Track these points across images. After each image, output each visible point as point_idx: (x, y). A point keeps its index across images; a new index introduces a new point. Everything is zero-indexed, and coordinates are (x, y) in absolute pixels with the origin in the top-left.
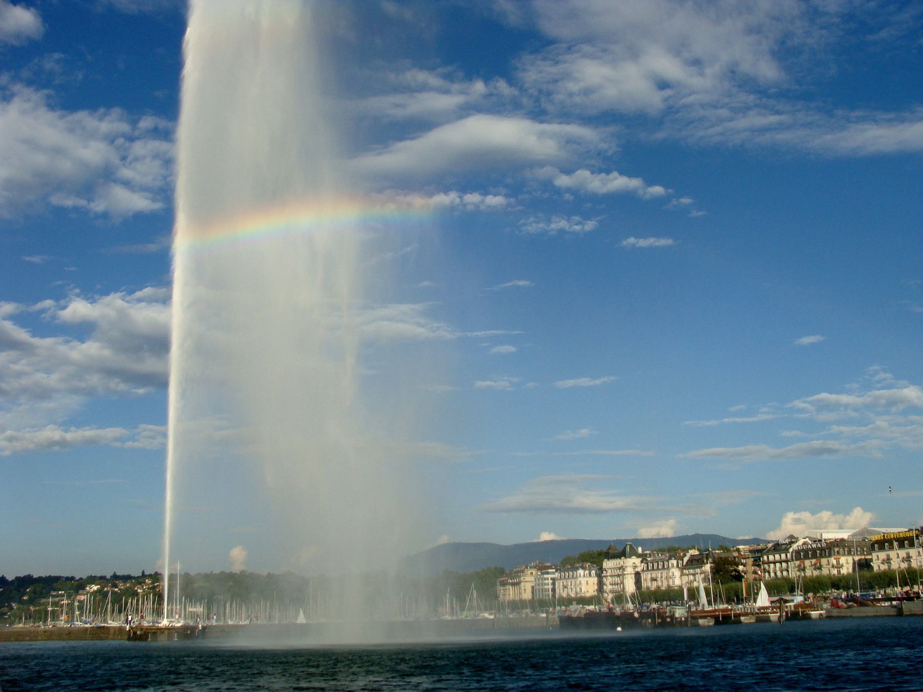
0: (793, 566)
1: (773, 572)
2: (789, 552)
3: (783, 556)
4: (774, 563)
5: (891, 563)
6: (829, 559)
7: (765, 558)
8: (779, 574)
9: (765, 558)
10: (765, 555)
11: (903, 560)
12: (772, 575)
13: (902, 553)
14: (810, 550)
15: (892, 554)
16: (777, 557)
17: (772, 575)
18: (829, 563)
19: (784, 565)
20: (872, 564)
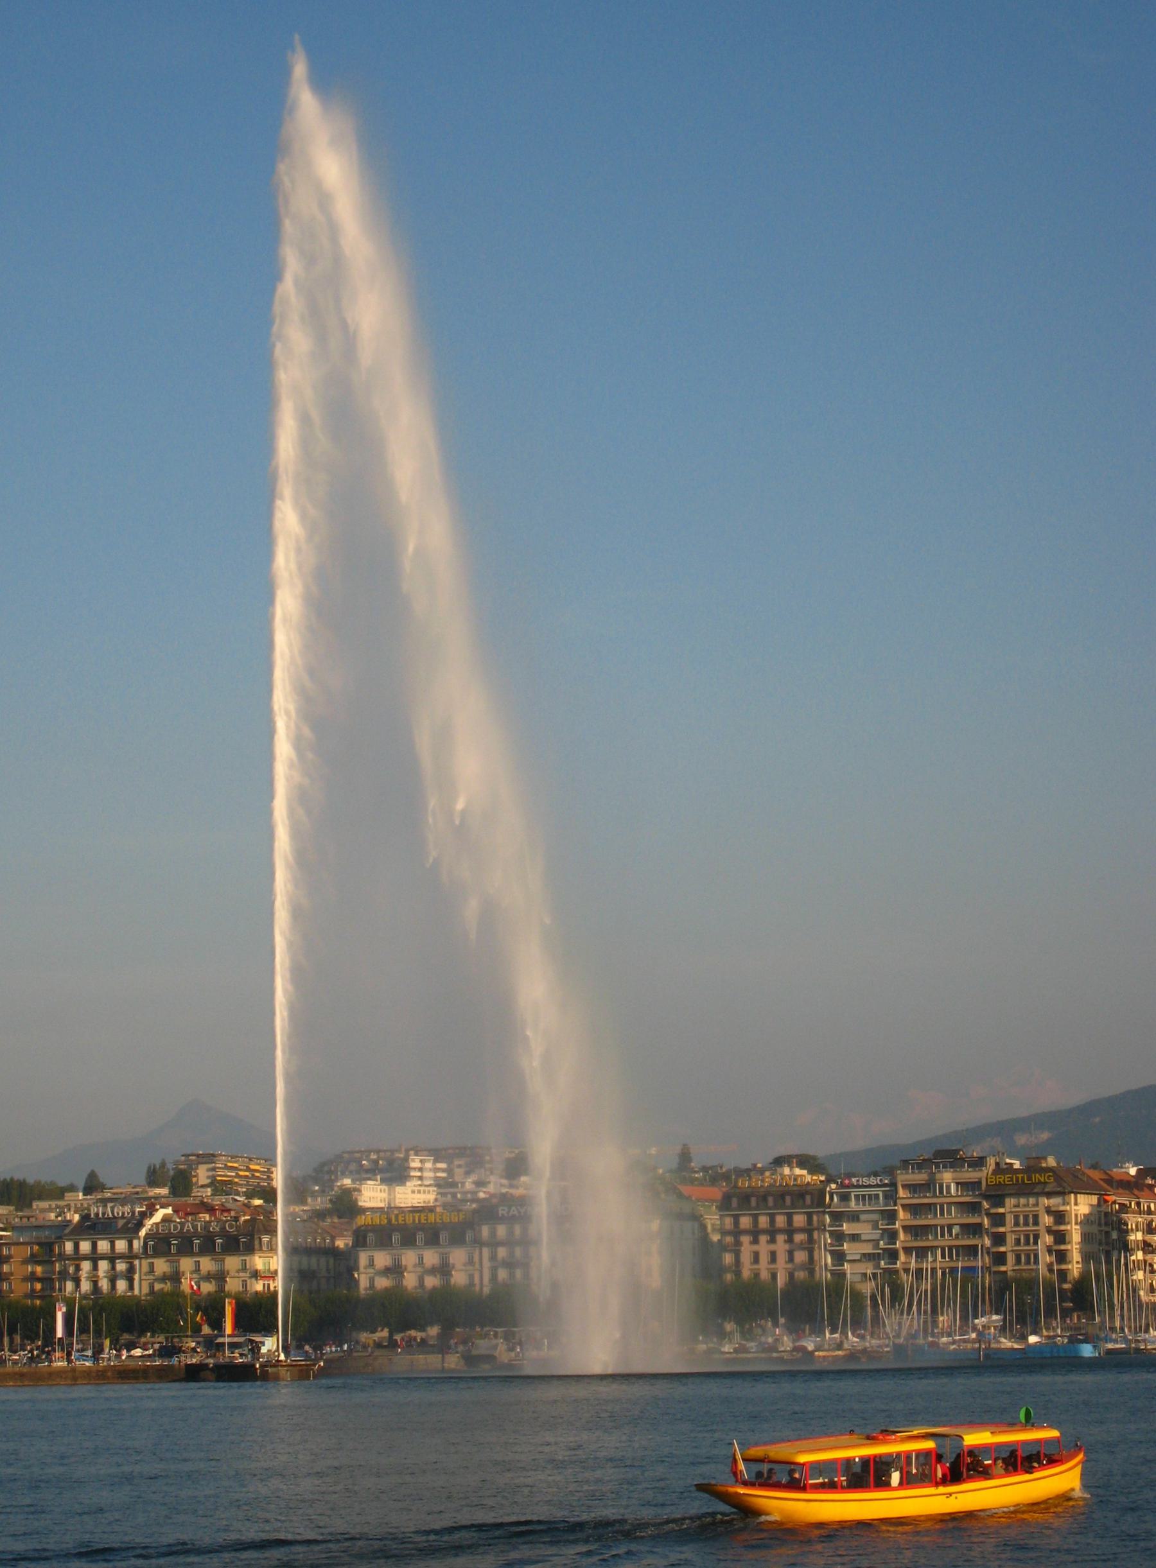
0: (145, 1268)
1: (88, 1278)
2: (139, 1238)
3: (121, 1245)
4: (94, 1258)
5: (404, 1276)
6: (247, 1258)
7: (69, 1246)
8: (104, 1284)
9: (69, 1246)
10: (69, 1240)
11: (387, 1271)
12: (86, 1286)
13: (431, 1257)
14: (196, 1234)
15: (409, 1257)
16: (103, 1246)
17: (86, 1286)
18: (244, 1269)
19: (121, 1266)
20: (356, 1276)
